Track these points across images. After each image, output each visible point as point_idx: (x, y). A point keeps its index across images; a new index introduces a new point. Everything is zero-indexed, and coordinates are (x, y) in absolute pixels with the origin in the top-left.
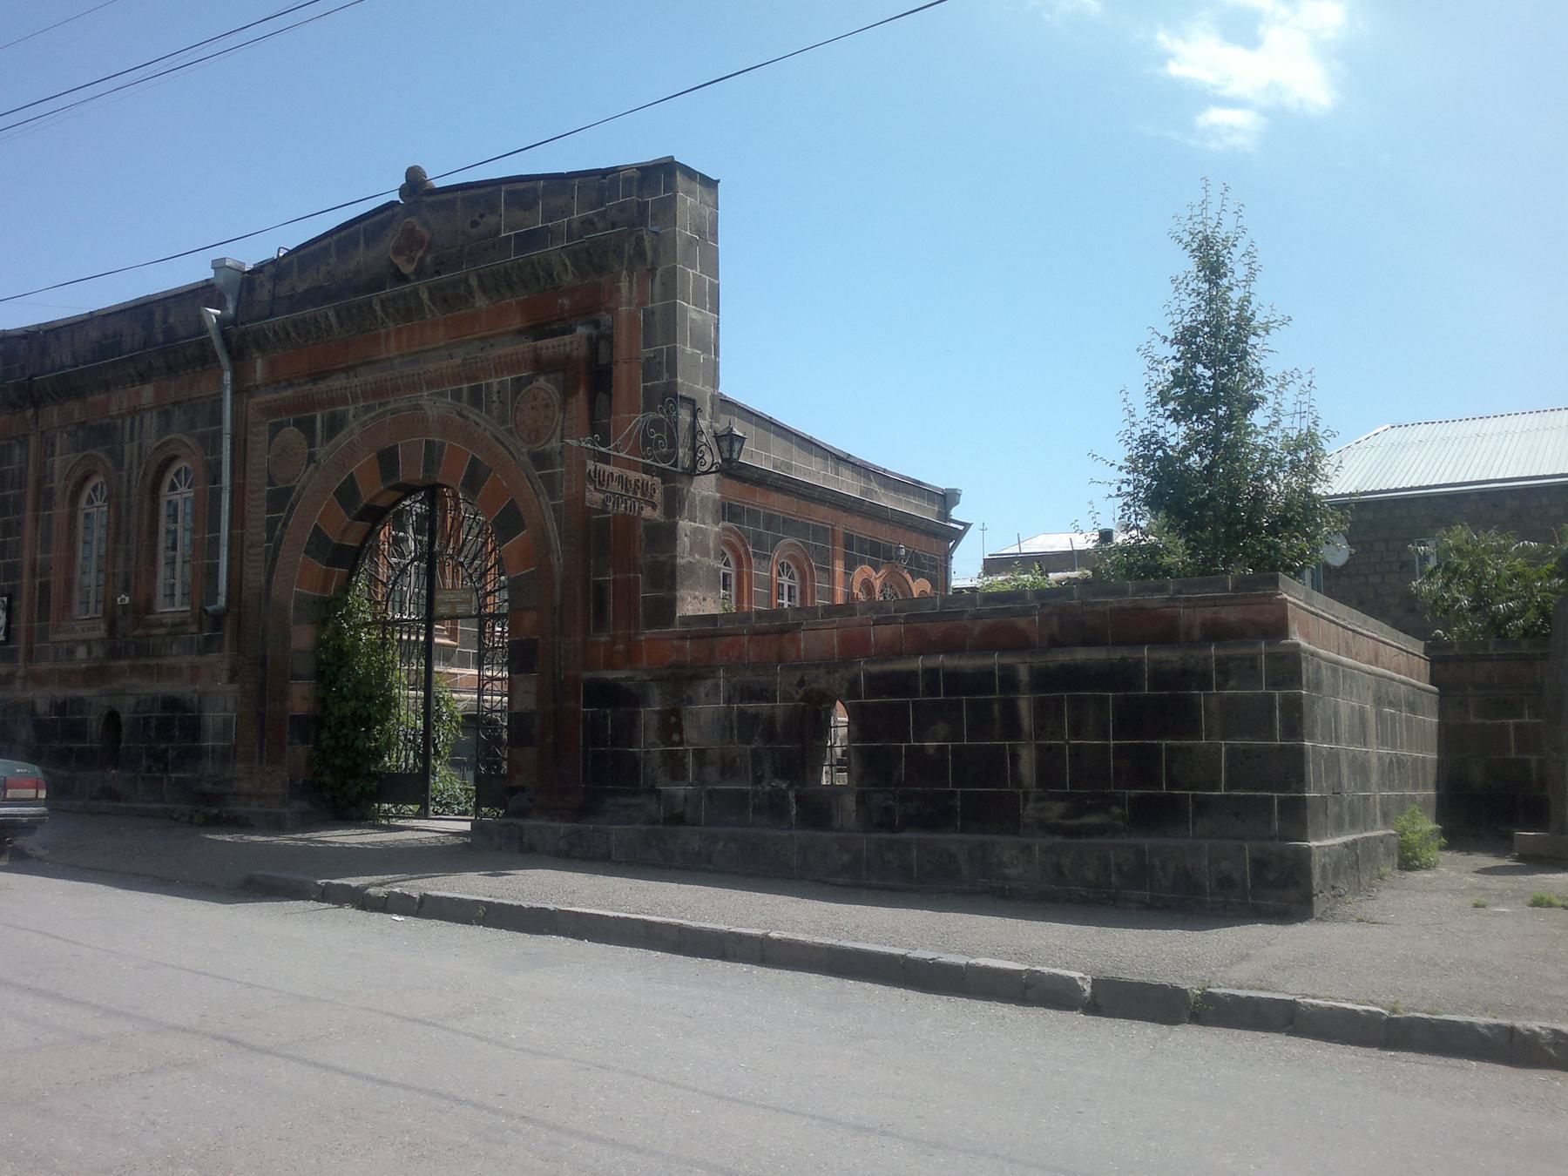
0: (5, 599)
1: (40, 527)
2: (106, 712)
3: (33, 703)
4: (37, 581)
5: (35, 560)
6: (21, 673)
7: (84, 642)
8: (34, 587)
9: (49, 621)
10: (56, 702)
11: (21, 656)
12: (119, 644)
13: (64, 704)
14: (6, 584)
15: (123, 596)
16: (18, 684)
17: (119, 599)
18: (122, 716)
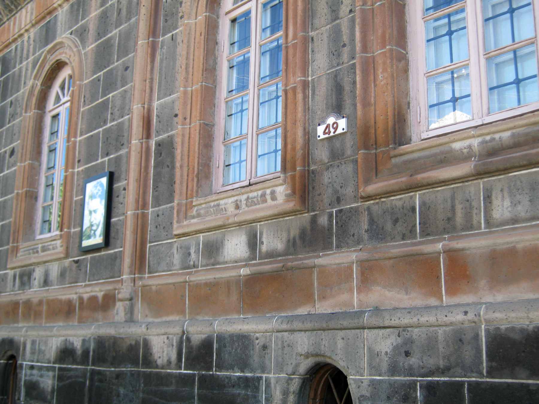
0: (104, 181)
1: (158, 58)
2: (305, 365)
3: (147, 344)
4: (153, 143)
5: (149, 111)
6: (125, 291)
7: (240, 224)
8: (148, 149)
9: (172, 201)
10: (188, 339)
11: (127, 261)
12: (323, 220)
13: (207, 345)
14: (106, 159)
15: (331, 120)
16: (120, 308)
17: (320, 130)
18: (351, 379)
